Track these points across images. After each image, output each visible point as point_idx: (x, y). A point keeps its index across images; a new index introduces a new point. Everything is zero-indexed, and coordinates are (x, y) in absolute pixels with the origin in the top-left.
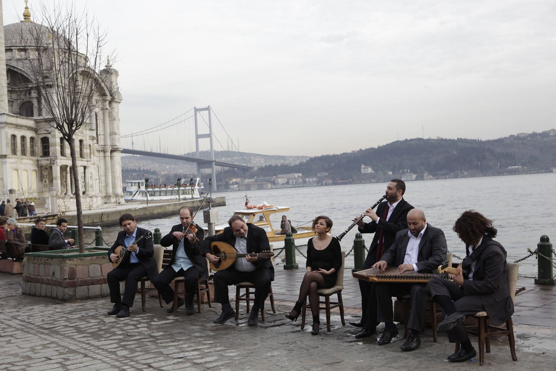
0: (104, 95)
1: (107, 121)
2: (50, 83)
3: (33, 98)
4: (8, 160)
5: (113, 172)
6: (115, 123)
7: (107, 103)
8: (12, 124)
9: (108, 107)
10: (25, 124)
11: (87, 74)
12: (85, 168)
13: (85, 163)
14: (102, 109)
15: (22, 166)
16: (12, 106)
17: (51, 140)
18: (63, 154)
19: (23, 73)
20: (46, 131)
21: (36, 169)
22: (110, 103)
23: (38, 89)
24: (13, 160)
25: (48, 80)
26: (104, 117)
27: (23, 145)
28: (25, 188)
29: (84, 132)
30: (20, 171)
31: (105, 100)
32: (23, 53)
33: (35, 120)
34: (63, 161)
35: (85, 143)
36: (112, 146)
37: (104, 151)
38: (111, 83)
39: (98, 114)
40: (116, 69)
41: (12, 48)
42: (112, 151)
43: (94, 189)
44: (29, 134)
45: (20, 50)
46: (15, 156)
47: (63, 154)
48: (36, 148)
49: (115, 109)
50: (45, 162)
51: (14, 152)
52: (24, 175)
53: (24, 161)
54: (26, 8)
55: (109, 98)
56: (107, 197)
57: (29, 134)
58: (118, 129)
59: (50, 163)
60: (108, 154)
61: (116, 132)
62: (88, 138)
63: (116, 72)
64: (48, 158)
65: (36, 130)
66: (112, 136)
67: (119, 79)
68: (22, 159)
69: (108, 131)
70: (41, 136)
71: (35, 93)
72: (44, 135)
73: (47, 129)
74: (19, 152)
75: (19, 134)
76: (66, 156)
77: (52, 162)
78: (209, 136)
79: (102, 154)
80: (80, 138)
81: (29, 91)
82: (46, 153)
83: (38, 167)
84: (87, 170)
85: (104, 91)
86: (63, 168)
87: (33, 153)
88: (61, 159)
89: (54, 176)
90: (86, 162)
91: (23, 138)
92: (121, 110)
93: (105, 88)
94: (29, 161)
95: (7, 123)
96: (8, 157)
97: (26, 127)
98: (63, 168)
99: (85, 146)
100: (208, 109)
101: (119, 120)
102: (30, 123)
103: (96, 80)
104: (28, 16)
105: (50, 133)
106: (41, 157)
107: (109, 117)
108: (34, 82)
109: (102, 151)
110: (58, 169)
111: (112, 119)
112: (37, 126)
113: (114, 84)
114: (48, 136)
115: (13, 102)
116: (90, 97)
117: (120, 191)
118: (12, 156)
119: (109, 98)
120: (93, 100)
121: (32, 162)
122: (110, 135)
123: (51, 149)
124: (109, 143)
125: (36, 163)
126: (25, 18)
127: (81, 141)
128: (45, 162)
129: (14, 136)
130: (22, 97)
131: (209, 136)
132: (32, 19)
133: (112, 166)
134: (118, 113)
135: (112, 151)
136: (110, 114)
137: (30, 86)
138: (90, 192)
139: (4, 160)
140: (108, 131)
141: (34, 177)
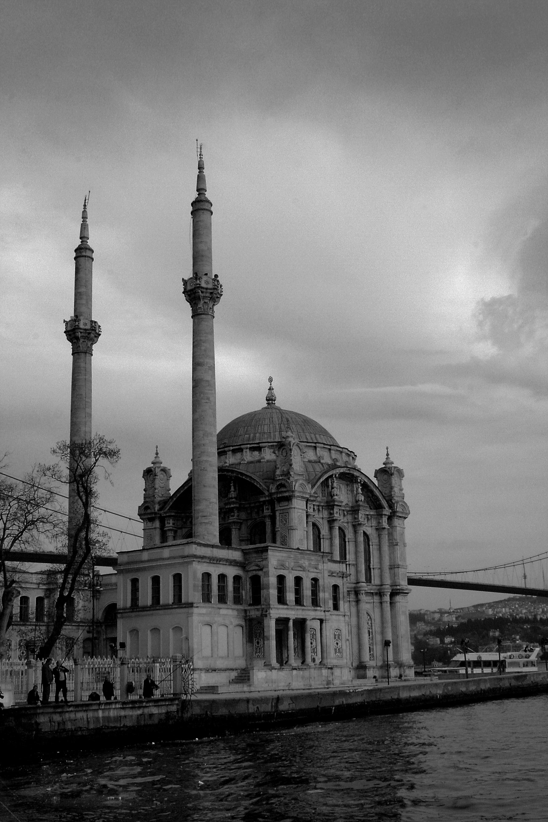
2: (287, 494)
3: (265, 517)
4: (195, 610)
6: (398, 550)
7: (385, 519)
8: (203, 557)
9: (385, 524)
10: (227, 557)
11: (350, 477)
12: (322, 621)
13: (320, 614)
14: (377, 529)
15: (219, 619)
16: (239, 529)
17: (263, 580)
18: (281, 600)
19: (253, 482)
20: (257, 566)
21: (243, 623)
22: (390, 518)
23: (272, 503)
24: (204, 611)
25: (283, 489)
26: (380, 541)
27: (222, 588)
28: (222, 650)
29: (320, 567)
30: (214, 627)
31: (381, 515)
32: (256, 453)
33: (243, 551)
35: (321, 582)
36: (393, 585)
37: (380, 594)
38: (392, 488)
39: (370, 537)
40: (401, 467)
41: (242, 446)
42: (393, 594)
43: (344, 654)
44: (231, 572)
45: (253, 449)
46: (207, 605)
47: (281, 600)
48: (243, 592)
49: (398, 528)
50: (254, 613)
51: (207, 598)
52: (222, 632)
53: (223, 612)
54: (269, 389)
55: (387, 511)
56: (386, 666)
57: (231, 572)
58: (404, 559)
59: (262, 615)
60: (387, 598)
61: (400, 563)
62: (326, 574)
63: (400, 472)
64: (259, 607)
65: (242, 565)
66: (392, 571)
67: (405, 483)
68: (220, 608)
70: (250, 574)
71: (268, 509)
73: (259, 563)
74: (214, 599)
75: (215, 571)
76: (287, 604)
77: (265, 615)
79: (376, 599)
80: (313, 575)
83: (246, 620)
84: (324, 624)
85: (379, 500)
87: (237, 600)
88: (278, 609)
89: (265, 634)
90: (323, 613)
91: (222, 577)
92: (411, 529)
93: (380, 497)
94: (230, 612)
95: (195, 556)
96: (195, 605)
97: (227, 560)
98: (282, 622)
99: (321, 588)
101: (405, 545)
103: (365, 487)
104: (272, 400)
105: (261, 570)
106: (250, 605)
107: (389, 540)
108: (267, 493)
109: (376, 594)
110: (273, 623)
111: (393, 544)
112: (245, 559)
113: (396, 489)
114: (260, 573)
115: (241, 523)
116: (354, 510)
118: (202, 605)
119: (387, 511)
120: (360, 515)
121: (235, 613)
122: (390, 569)
123: (263, 592)
124: (388, 581)
125: (243, 614)
126: (268, 404)
129: (207, 576)
130: (254, 515)
132: (277, 403)
133: (394, 617)
134: (402, 534)
135: (393, 594)
136: (390, 534)
137: (262, 499)
138: (329, 661)
139: (190, 610)
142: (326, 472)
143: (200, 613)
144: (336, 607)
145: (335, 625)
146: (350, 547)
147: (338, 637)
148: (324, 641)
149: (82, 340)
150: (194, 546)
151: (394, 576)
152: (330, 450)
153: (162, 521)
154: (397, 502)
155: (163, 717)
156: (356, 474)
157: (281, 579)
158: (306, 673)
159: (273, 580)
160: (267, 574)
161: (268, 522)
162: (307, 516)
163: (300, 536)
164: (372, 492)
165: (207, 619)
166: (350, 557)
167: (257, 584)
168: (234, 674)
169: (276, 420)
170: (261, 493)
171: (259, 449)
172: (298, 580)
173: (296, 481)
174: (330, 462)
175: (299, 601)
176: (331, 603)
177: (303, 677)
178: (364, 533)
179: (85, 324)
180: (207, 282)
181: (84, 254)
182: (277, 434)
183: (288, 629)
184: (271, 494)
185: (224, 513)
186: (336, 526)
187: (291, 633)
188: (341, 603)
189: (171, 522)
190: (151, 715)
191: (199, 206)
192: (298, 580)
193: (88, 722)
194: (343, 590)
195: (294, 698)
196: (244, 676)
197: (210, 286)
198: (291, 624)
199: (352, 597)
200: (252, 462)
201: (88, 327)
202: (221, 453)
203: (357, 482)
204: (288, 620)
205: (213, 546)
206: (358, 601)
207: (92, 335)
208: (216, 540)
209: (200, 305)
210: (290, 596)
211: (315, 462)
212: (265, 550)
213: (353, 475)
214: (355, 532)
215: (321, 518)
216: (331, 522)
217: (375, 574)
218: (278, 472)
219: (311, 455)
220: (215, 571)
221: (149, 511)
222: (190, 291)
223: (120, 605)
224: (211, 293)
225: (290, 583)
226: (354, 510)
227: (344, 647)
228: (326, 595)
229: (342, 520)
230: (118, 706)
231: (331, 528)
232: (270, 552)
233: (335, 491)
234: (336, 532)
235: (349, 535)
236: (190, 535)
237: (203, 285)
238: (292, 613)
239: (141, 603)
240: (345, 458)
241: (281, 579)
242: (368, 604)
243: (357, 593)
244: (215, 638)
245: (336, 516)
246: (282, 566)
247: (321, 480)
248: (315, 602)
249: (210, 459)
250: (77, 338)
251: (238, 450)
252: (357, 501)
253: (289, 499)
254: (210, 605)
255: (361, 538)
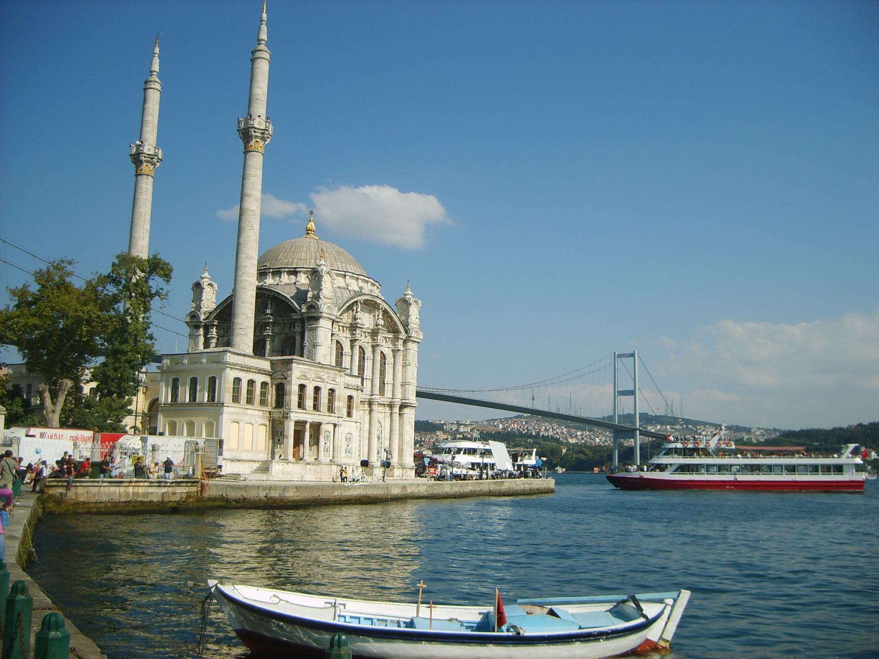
0: (396, 331)
1: (399, 367)
2: (315, 315)
5: (401, 434)
7: (401, 342)
9: (401, 347)
12: (335, 425)
13: (334, 420)
17: (287, 388)
18: (301, 405)
21: (267, 423)
22: (405, 342)
23: (302, 321)
24: (233, 410)
27: (250, 392)
28: (247, 445)
29: (337, 380)
31: (396, 339)
32: (293, 277)
34: (299, 415)
35: (337, 393)
42: (403, 406)
43: (353, 455)
44: (259, 379)
46: (235, 405)
47: (301, 405)
51: (236, 399)
53: (249, 412)
55: (403, 335)
57: (259, 379)
62: (342, 387)
69: (399, 379)
70: (276, 382)
72: (280, 381)
75: (245, 377)
77: (286, 416)
78: (632, 393)
79: (387, 409)
80: (331, 386)
81: (292, 324)
82: (280, 402)
84: (337, 428)
86: (300, 424)
91: (251, 383)
93: (398, 323)
97: (256, 368)
98: (300, 424)
100: (632, 355)
102: (265, 365)
103: (385, 312)
106: (276, 407)
114: (284, 381)
116: (374, 333)
117: (409, 461)
119: (403, 335)
122: (402, 385)
123: (287, 398)
124: (399, 395)
127: (332, 391)
128: (277, 413)
129: (237, 380)
130: (286, 330)
131: (632, 393)
133: (401, 426)
136: (405, 356)
140: (399, 379)
141: (262, 434)
142: (352, 298)
143: (230, 412)
144: (349, 414)
145: (347, 430)
146: (368, 364)
147: (349, 439)
148: (336, 442)
149: (145, 164)
150: (228, 354)
151: (404, 391)
152: (357, 279)
153: (207, 329)
154: (413, 328)
155: (184, 496)
156: (379, 301)
157: (302, 387)
158: (319, 468)
159: (295, 389)
160: (290, 383)
161: (298, 337)
162: (332, 335)
163: (325, 352)
164: (391, 318)
165: (235, 417)
166: (368, 373)
167: (281, 391)
168: (256, 465)
169: (312, 248)
170: (293, 310)
171: (294, 272)
172: (317, 389)
173: (325, 304)
174: (357, 289)
175: (316, 407)
176: (345, 411)
177: (315, 471)
178: (382, 352)
179: (149, 150)
180: (259, 123)
181: (153, 86)
182: (313, 261)
183: (304, 431)
184: (302, 314)
185: (259, 326)
186: (357, 344)
187: (307, 434)
188: (354, 412)
189: (215, 330)
190: (174, 493)
191: (258, 54)
192: (317, 389)
193: (120, 496)
194: (356, 401)
195: (298, 488)
196: (265, 468)
197: (263, 127)
198: (308, 426)
199: (366, 407)
200: (288, 284)
201: (152, 152)
202: (262, 274)
203: (379, 309)
204: (306, 422)
205: (245, 355)
206: (371, 411)
207: (155, 160)
208: (249, 350)
209: (253, 143)
210: (309, 403)
211: (344, 288)
212: (290, 362)
213: (376, 303)
214: (374, 352)
215: (345, 337)
216: (353, 341)
217: (388, 388)
218: (310, 295)
219: (340, 282)
220: (245, 377)
221: (195, 320)
222: (244, 129)
223: (163, 400)
224: (263, 133)
225: (310, 392)
226: (374, 333)
227: (354, 449)
228: (340, 404)
229: (365, 341)
230: (146, 484)
231: (352, 347)
232: (294, 365)
233: (359, 315)
234: (357, 350)
235: (369, 353)
236: (228, 344)
237: (256, 126)
238: (309, 416)
239: (180, 400)
240: (370, 287)
241: (302, 387)
242: (381, 414)
243: (370, 404)
244: (241, 434)
245: (358, 336)
246: (304, 377)
247: (347, 305)
248: (331, 409)
249: (250, 279)
250: (141, 162)
251: (277, 273)
252: (377, 325)
253: (317, 319)
254: (239, 405)
255: (378, 357)
